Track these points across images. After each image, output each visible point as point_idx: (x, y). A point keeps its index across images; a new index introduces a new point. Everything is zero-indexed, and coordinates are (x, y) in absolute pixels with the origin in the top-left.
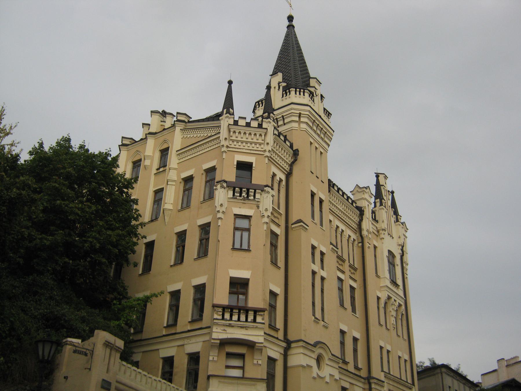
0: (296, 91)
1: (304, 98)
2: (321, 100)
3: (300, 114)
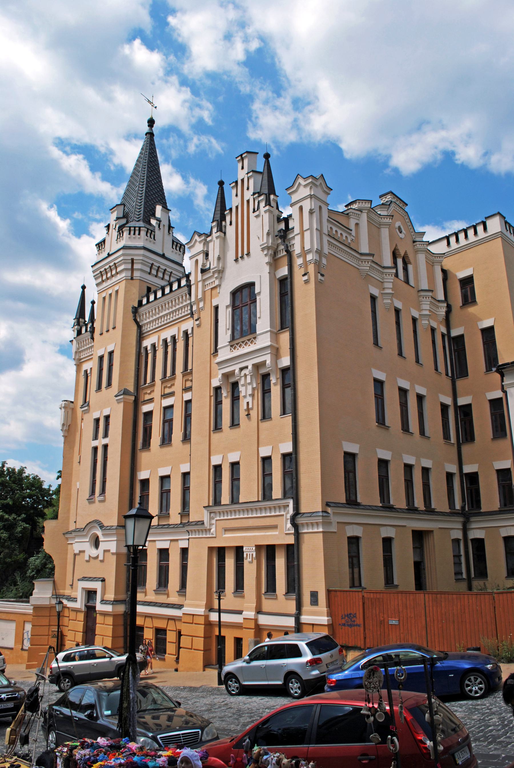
0: (130, 231)
1: (139, 238)
2: (169, 232)
3: (132, 260)
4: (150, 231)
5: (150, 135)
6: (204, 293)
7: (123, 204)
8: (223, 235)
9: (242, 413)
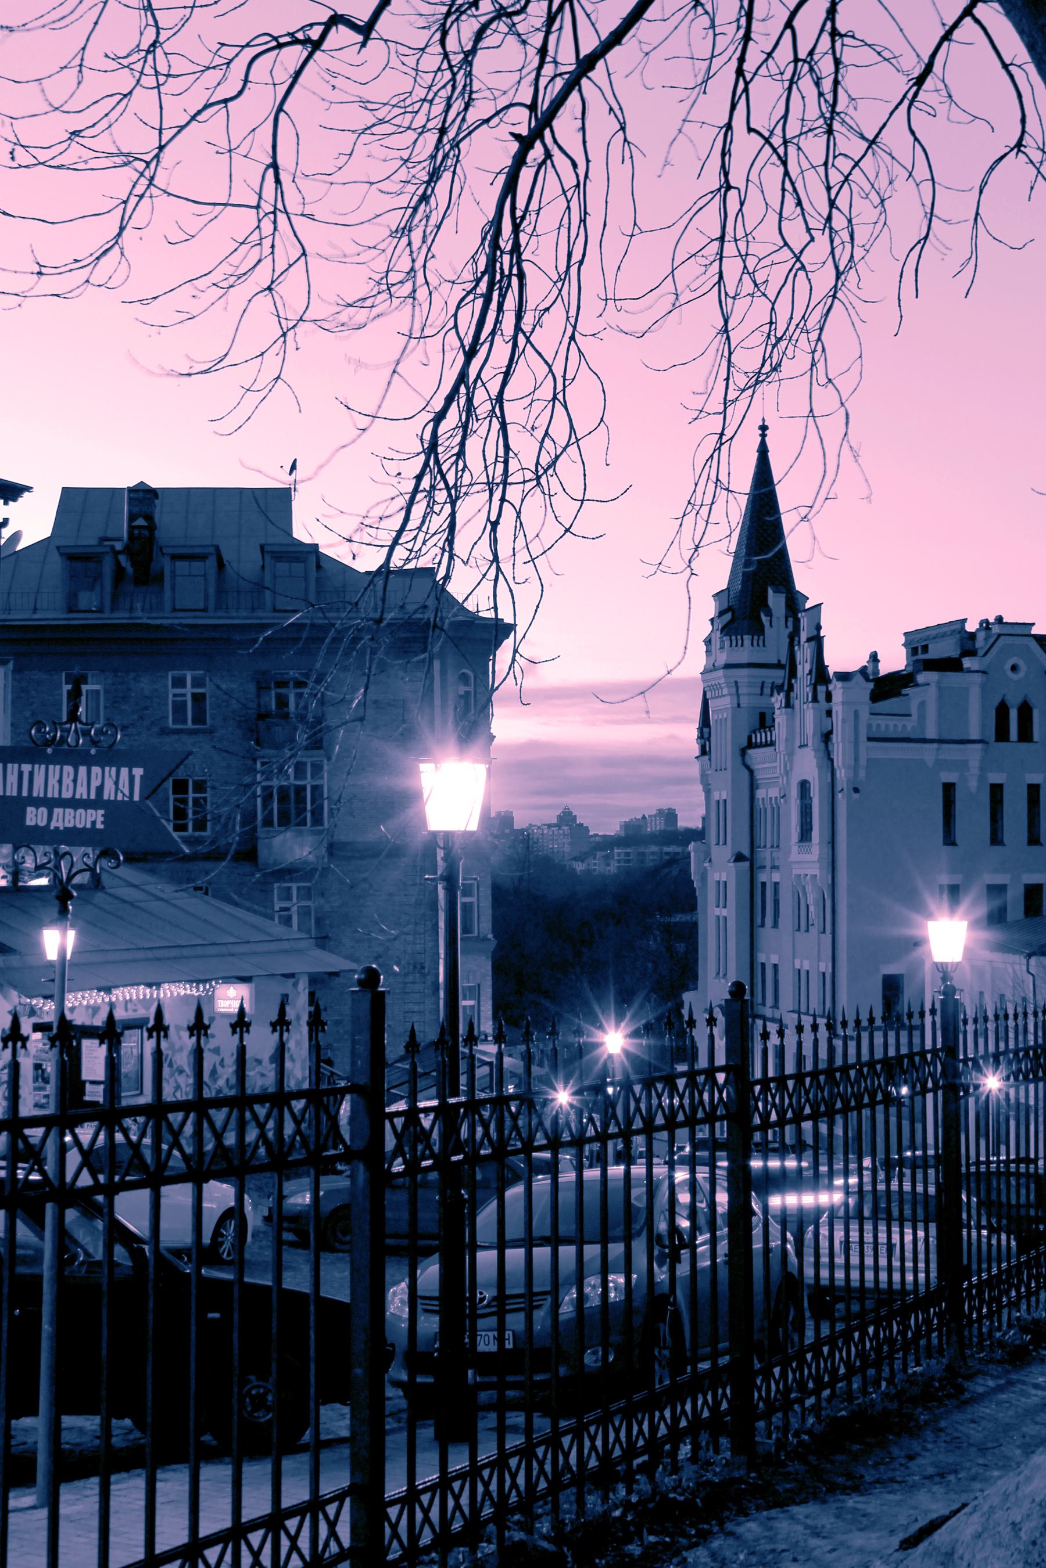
2: (786, 626)
3: (736, 682)
4: (756, 637)
5: (763, 451)
6: (785, 766)
7: (728, 588)
8: (789, 710)
9: (810, 923)
